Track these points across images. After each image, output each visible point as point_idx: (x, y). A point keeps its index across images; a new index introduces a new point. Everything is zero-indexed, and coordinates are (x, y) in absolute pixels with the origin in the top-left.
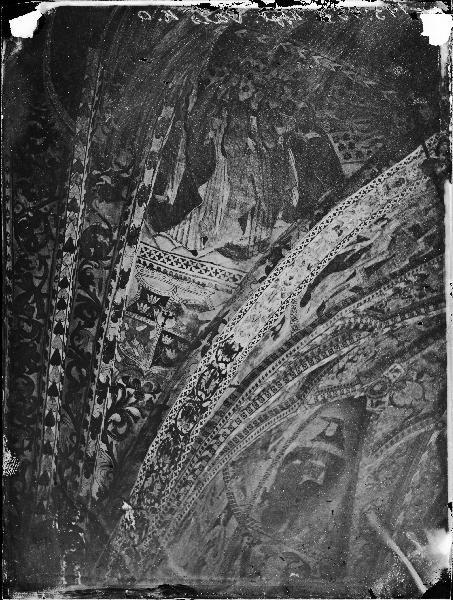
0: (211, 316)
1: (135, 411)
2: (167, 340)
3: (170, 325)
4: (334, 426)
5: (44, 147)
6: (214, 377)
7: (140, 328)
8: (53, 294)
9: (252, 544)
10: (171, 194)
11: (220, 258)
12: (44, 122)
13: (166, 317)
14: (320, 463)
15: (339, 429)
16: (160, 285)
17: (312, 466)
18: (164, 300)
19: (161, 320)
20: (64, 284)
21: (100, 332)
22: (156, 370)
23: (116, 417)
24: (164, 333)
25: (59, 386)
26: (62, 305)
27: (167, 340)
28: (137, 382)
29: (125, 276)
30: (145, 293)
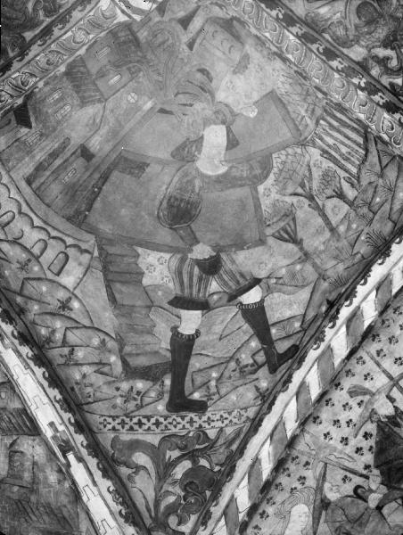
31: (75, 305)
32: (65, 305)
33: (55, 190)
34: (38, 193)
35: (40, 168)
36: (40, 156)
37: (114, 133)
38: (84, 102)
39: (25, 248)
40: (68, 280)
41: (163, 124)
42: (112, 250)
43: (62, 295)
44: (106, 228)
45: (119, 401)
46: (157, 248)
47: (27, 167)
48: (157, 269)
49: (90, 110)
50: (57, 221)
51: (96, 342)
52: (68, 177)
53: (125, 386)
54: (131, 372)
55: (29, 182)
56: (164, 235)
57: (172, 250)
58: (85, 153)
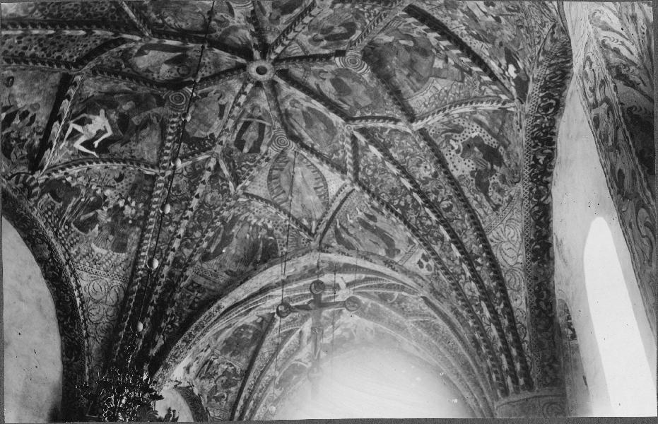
0: (215, 294)
1: (177, 324)
2: (197, 300)
3: (199, 295)
4: (260, 319)
5: (168, 225)
6: (210, 316)
7: (187, 295)
8: (157, 279)
9: (214, 359)
10: (212, 249)
11: (225, 274)
12: (170, 218)
13: (199, 292)
14: (251, 331)
15: (262, 321)
16: (201, 281)
17: (248, 333)
18: (199, 286)
19: (196, 293)
20: (163, 277)
21: (172, 294)
22: (189, 311)
23: (170, 326)
24: (196, 297)
25: (151, 314)
26: (160, 285)
27: (197, 300)
28: (181, 314)
29: (187, 277)
30: (192, 282)
31: (446, 88)
32: (446, 91)
33: (418, 85)
34: (418, 89)
35: (412, 88)
36: (409, 88)
37: (403, 67)
38: (395, 75)
39: (431, 97)
40: (440, 88)
41: (401, 54)
42: (433, 74)
43: (443, 91)
44: (428, 74)
45: (469, 87)
46: (433, 62)
47: (412, 91)
48: (439, 64)
49: (397, 74)
50: (426, 86)
51: (455, 87)
52: (415, 81)
53: (466, 84)
54: (462, 81)
55: (415, 92)
56: (430, 58)
57: (434, 58)
58: (408, 76)
